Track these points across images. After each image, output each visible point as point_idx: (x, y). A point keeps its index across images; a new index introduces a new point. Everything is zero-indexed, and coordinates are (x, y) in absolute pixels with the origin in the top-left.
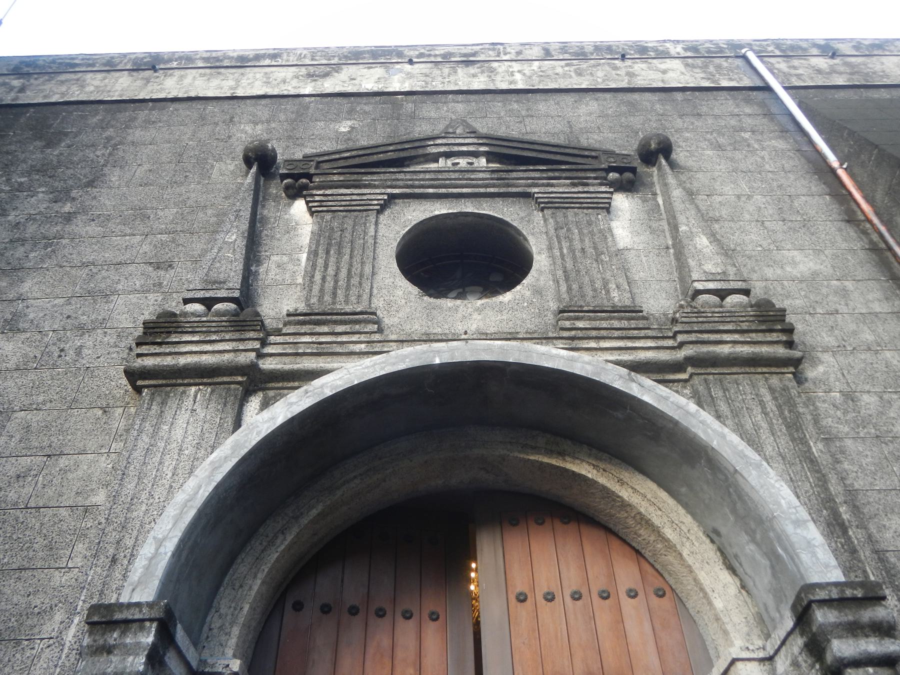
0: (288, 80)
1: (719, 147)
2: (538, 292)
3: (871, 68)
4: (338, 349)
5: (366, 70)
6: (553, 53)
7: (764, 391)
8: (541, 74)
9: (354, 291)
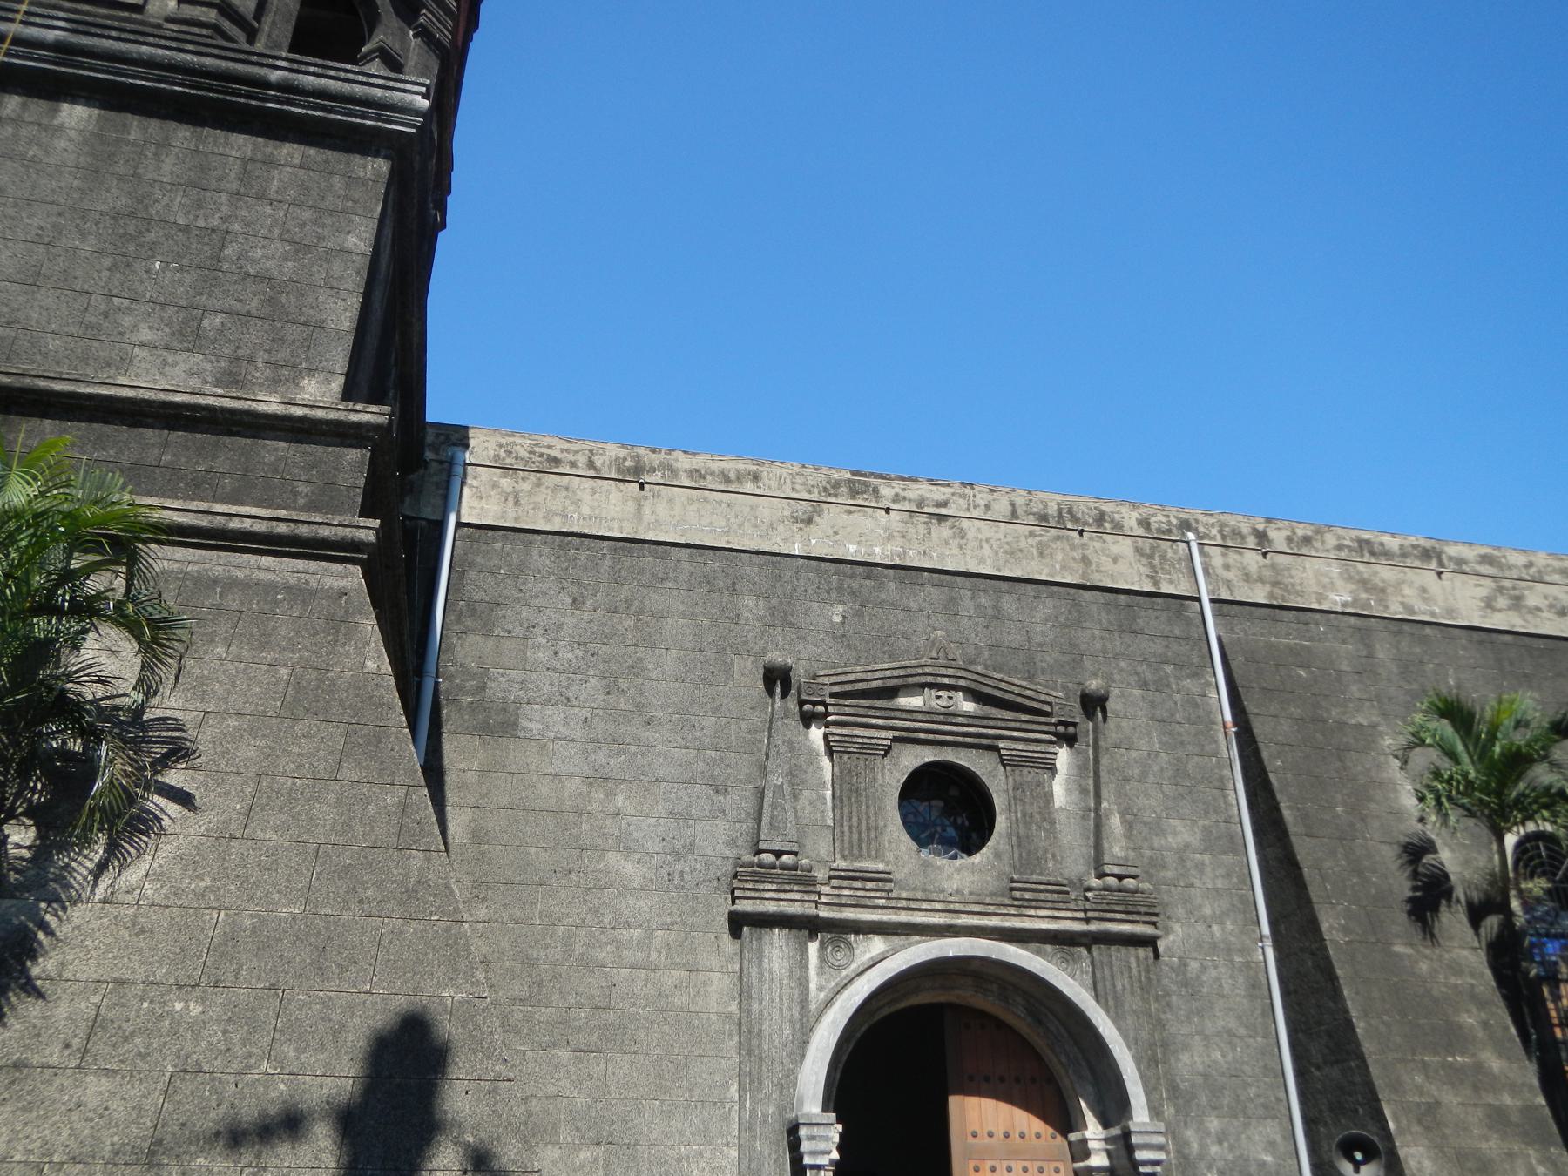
0: (775, 525)
1: (1144, 685)
2: (997, 855)
3: (1292, 577)
4: (868, 902)
5: (845, 516)
6: (1019, 512)
7: (1133, 960)
8: (1006, 547)
9: (873, 845)
